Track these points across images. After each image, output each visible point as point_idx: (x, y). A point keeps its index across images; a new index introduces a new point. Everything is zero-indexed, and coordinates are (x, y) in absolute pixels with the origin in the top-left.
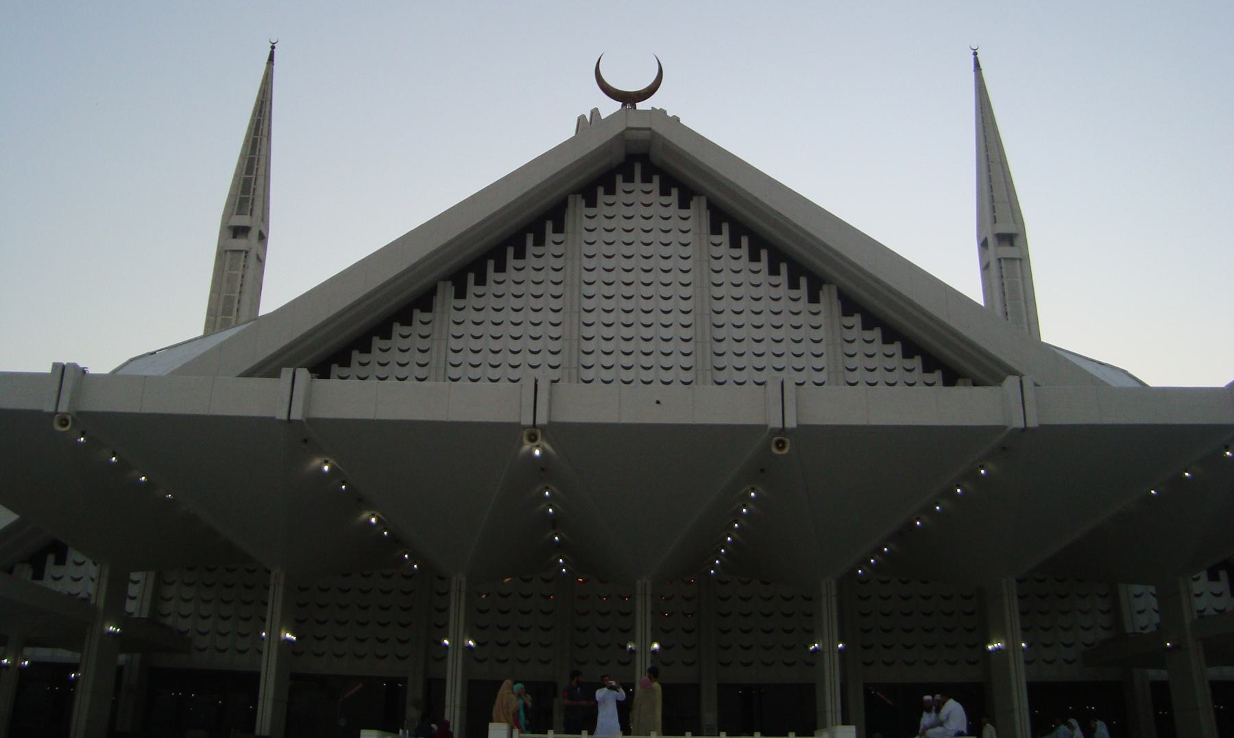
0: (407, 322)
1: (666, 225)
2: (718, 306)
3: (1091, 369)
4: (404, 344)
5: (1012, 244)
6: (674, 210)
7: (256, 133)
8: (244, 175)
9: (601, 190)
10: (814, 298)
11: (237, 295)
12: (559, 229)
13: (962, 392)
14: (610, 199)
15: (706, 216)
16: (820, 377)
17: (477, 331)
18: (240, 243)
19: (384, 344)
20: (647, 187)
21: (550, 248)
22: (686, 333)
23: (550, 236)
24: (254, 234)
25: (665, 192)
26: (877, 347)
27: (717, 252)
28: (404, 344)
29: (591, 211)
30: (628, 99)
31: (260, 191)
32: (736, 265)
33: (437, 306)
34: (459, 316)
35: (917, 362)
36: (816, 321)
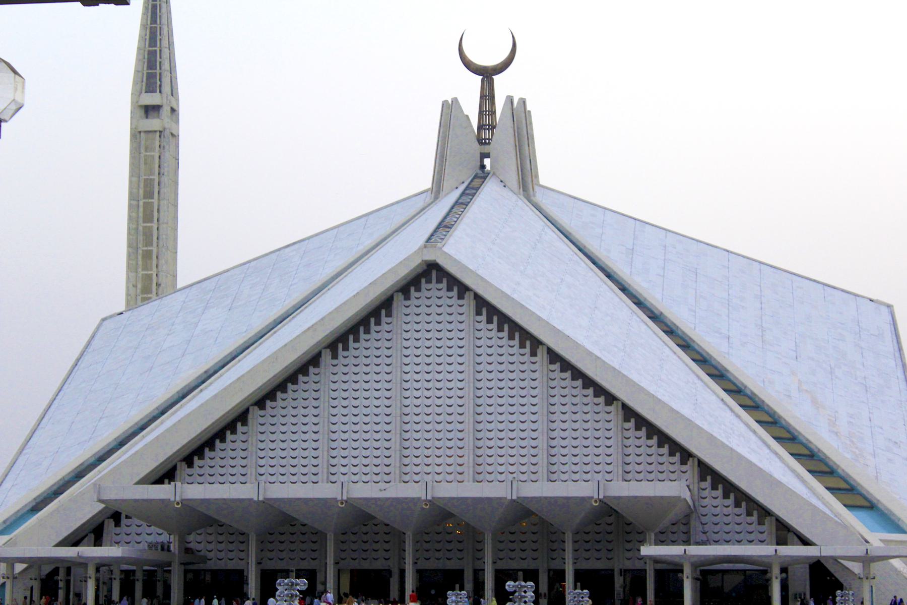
1: (449, 310)
2: (478, 360)
4: (306, 387)
6: (455, 301)
8: (147, 48)
9: (412, 289)
10: (533, 354)
11: (156, 177)
12: (389, 315)
14: (417, 294)
15: (473, 303)
17: (345, 378)
18: (154, 124)
19: (294, 387)
20: (440, 286)
21: (385, 327)
23: (384, 319)
24: (166, 110)
25: (449, 289)
26: (569, 382)
27: (479, 326)
28: (306, 387)
29: (407, 303)
30: (487, 74)
31: (166, 66)
32: (490, 334)
33: (322, 364)
34: (335, 370)
35: (590, 391)
36: (533, 367)
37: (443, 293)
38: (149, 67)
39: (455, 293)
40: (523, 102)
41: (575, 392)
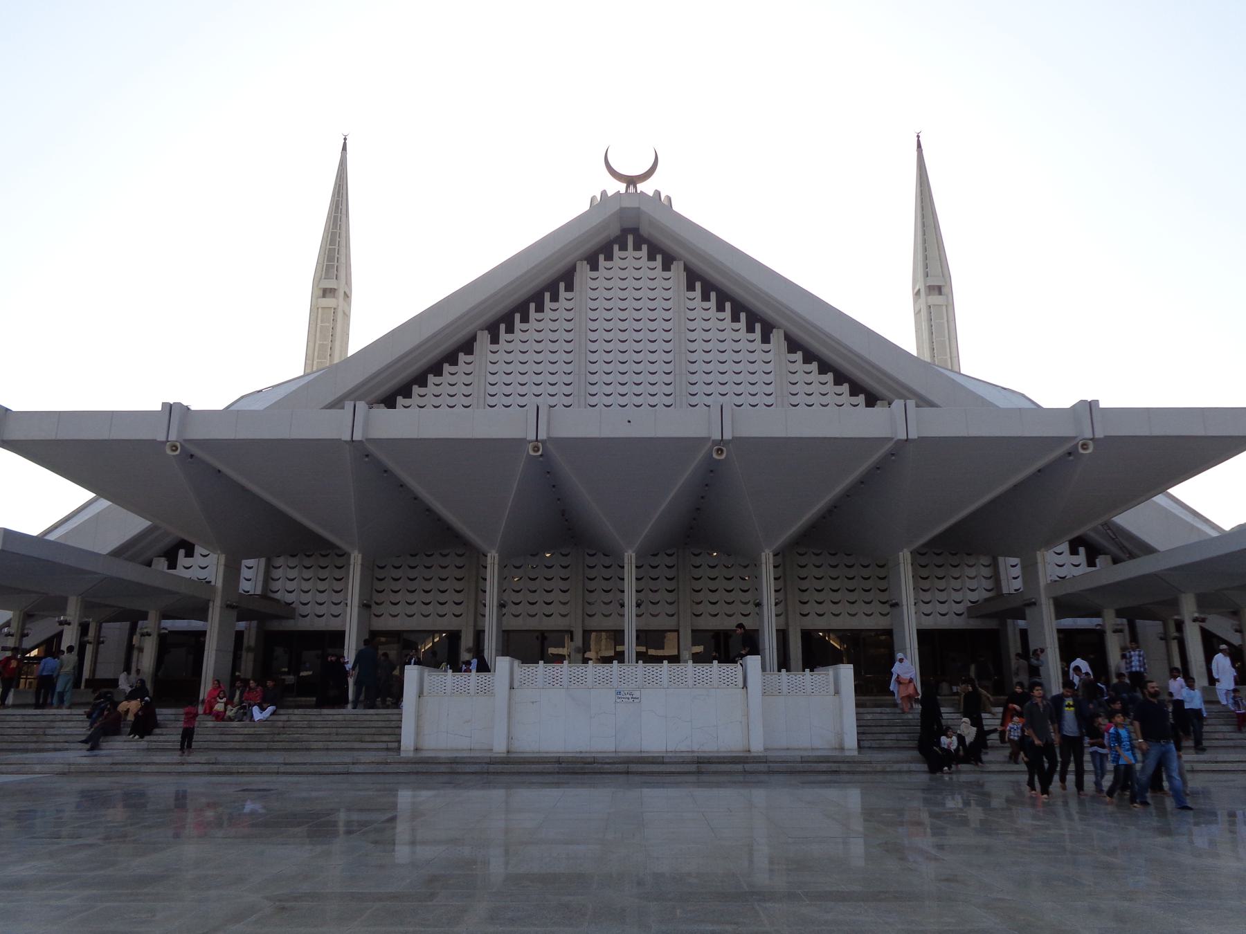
0: (454, 362)
3: (981, 391)
5: (940, 293)
7: (336, 212)
9: (601, 257)
10: (766, 339)
12: (569, 288)
13: (879, 410)
14: (609, 264)
15: (683, 275)
16: (769, 400)
18: (329, 302)
20: (637, 254)
21: (563, 303)
22: (668, 368)
23: (563, 294)
25: (651, 257)
26: (815, 377)
27: (691, 305)
28: (453, 379)
29: (594, 274)
30: (631, 181)
31: (343, 260)
36: (767, 357)
37: (644, 262)
38: (329, 260)
39: (658, 262)
40: (669, 199)
41: (824, 389)
